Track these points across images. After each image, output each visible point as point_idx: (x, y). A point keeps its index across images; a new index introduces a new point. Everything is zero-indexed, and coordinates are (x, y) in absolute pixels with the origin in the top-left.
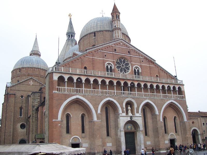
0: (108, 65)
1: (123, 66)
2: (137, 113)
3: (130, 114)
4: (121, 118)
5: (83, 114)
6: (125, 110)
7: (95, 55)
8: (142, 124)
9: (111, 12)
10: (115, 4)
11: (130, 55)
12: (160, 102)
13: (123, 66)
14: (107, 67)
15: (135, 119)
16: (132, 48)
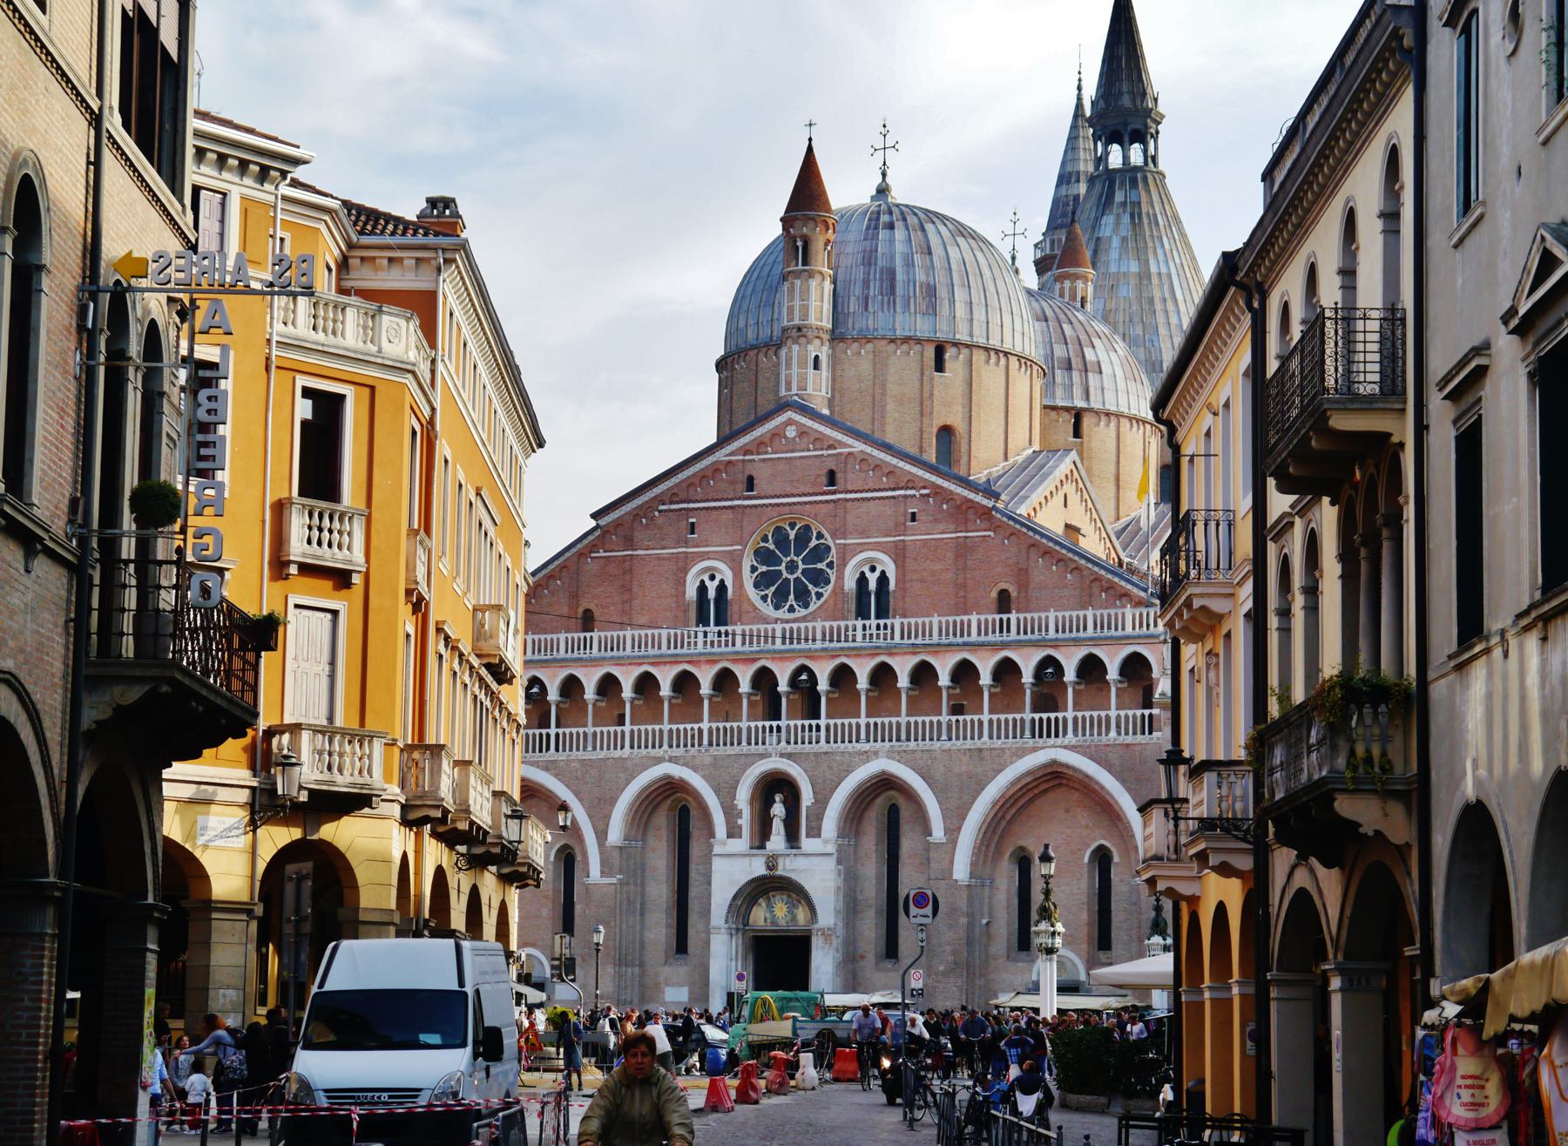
0: (706, 578)
1: (793, 566)
2: (808, 836)
3: (777, 842)
4: (718, 865)
5: (565, 847)
6: (745, 821)
7: (638, 535)
8: (831, 897)
9: (782, 214)
10: (810, 149)
11: (834, 493)
12: (964, 769)
13: (792, 567)
14: (702, 589)
15: (793, 870)
16: (851, 447)
